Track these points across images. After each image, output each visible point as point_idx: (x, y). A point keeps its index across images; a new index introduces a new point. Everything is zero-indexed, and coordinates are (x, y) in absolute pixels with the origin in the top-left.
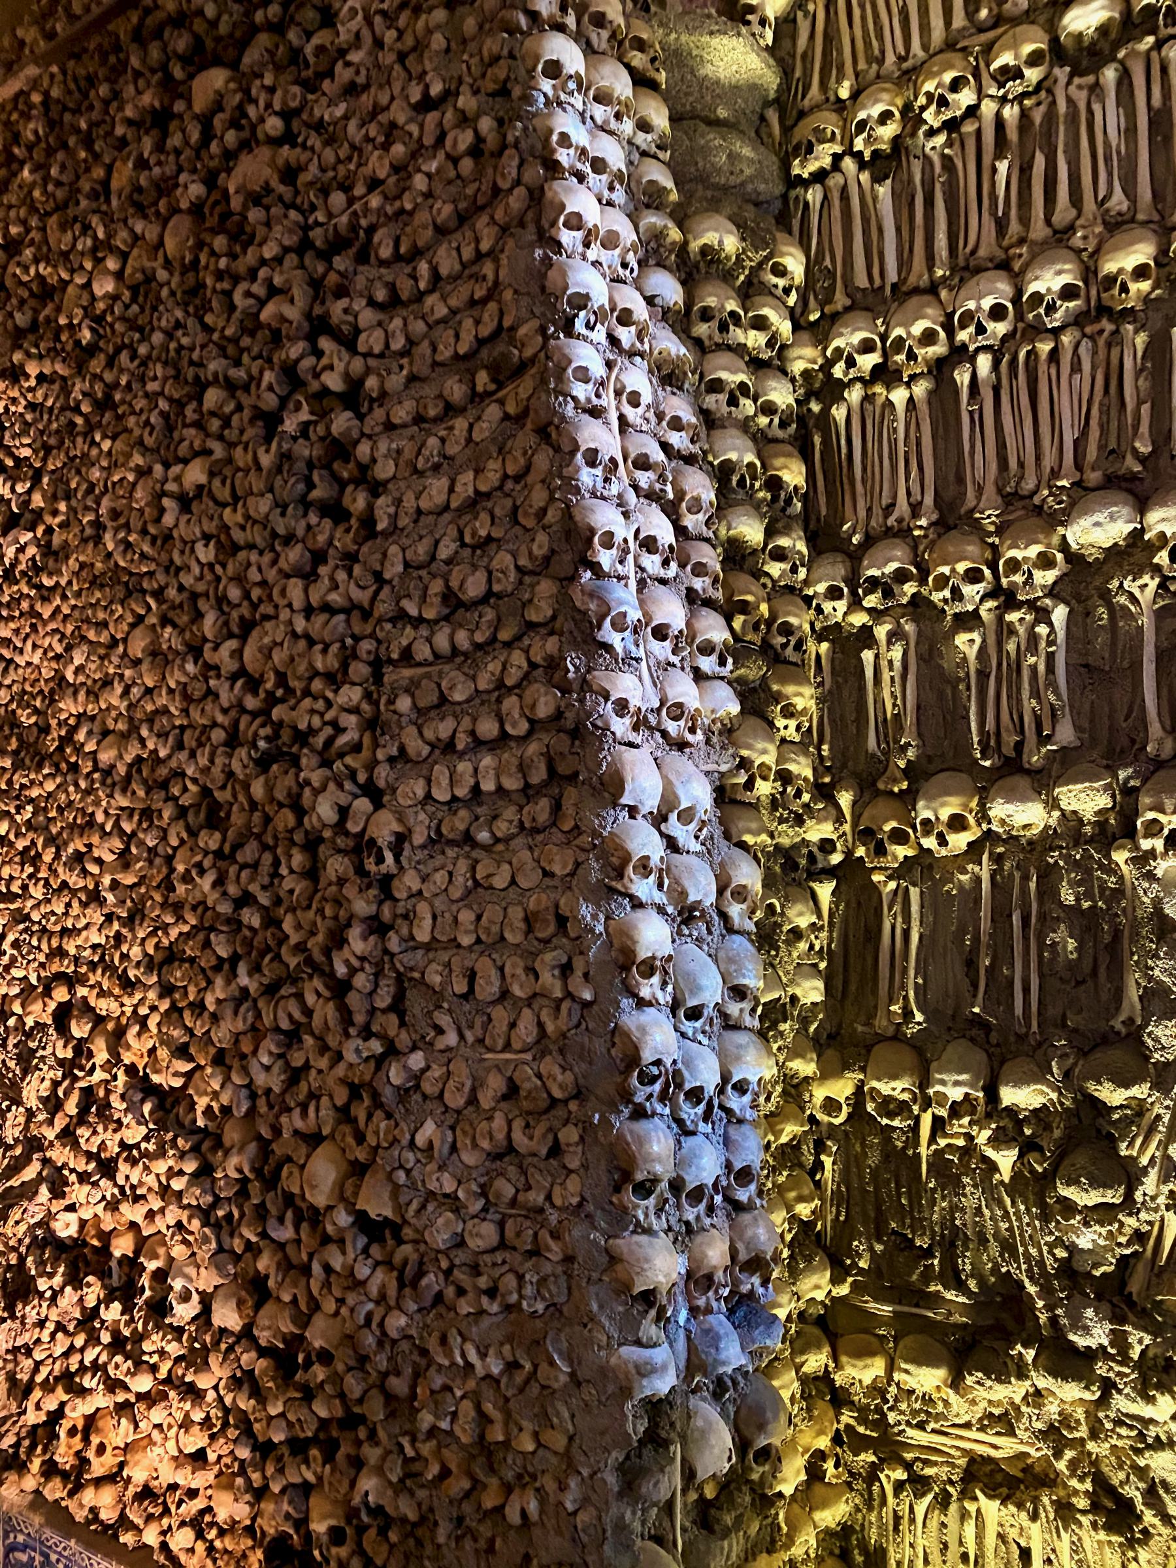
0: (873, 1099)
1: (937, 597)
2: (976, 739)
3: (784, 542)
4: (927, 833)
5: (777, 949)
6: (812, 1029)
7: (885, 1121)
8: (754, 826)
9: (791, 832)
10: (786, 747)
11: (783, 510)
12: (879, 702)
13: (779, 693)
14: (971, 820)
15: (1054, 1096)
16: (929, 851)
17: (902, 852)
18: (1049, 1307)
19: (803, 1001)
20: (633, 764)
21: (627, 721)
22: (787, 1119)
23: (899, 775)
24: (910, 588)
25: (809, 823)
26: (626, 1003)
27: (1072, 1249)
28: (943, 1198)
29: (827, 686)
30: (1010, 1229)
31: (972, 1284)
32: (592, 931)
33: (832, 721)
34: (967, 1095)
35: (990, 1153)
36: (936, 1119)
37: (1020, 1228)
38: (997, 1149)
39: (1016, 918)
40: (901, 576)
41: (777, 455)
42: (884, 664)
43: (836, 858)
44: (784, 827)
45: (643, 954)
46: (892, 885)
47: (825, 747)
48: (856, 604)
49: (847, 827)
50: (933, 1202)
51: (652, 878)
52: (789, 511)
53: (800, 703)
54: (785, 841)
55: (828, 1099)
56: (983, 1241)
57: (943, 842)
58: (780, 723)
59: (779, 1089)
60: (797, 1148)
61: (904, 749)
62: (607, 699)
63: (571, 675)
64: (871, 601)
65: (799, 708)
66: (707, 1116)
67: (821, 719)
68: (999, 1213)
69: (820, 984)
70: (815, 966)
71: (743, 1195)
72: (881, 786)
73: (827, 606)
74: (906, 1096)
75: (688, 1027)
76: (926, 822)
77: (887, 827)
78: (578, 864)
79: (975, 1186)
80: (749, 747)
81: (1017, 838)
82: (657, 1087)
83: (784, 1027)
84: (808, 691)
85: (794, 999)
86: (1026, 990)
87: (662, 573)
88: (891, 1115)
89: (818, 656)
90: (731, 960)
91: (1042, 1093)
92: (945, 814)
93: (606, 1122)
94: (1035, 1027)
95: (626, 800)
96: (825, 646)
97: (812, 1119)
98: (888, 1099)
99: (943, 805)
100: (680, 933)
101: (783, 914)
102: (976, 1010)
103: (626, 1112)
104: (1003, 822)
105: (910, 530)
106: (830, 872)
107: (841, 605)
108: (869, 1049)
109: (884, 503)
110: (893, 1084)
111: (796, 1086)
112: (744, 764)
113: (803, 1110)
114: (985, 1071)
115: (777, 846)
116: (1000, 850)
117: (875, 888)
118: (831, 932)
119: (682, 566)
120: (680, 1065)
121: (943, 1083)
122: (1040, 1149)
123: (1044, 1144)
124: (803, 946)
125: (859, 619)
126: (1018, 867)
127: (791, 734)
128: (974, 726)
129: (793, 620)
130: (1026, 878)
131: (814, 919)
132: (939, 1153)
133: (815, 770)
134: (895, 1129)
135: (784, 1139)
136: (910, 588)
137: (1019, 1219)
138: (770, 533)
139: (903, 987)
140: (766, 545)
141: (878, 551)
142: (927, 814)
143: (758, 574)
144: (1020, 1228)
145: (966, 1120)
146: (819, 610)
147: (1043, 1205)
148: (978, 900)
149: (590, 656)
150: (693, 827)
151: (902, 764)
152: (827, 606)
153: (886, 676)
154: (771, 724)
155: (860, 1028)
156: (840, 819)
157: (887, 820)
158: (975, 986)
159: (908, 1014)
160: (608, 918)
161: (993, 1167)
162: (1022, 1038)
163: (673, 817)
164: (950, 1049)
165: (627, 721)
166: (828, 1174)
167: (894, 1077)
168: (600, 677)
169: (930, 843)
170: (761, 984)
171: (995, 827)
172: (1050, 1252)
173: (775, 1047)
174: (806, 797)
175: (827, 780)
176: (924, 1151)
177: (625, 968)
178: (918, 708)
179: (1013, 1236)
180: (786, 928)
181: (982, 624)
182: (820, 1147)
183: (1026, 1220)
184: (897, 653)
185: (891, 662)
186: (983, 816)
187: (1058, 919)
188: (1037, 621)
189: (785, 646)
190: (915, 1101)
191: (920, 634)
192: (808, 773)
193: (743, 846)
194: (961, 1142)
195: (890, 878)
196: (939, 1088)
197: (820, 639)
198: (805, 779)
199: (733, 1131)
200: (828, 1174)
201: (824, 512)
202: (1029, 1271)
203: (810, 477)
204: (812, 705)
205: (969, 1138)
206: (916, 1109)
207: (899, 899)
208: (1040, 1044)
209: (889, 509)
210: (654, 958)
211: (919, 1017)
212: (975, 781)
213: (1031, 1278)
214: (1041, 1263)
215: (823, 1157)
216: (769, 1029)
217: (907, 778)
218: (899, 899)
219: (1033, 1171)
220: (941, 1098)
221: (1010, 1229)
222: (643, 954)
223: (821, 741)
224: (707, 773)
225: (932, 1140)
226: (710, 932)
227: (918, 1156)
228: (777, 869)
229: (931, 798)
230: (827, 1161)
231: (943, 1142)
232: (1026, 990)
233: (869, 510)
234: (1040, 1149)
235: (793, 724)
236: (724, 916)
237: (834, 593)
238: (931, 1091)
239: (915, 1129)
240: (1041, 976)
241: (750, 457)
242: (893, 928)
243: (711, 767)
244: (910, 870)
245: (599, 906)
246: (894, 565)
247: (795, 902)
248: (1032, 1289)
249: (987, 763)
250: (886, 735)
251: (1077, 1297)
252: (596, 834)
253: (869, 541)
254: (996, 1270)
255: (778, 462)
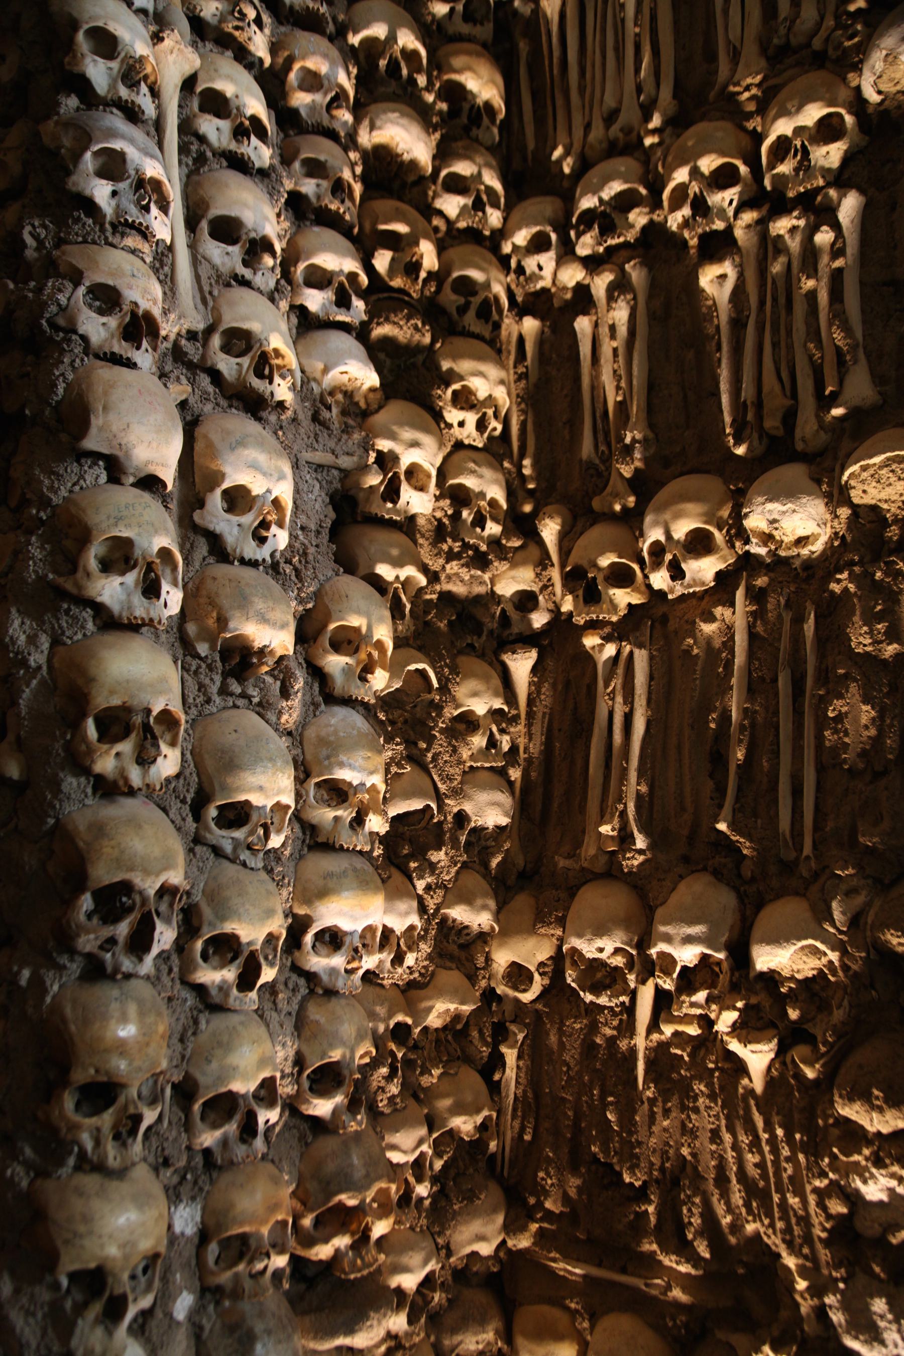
0: (574, 964)
1: (675, 220)
2: (728, 419)
3: (463, 168)
4: (657, 565)
5: (431, 740)
6: (495, 862)
7: (589, 997)
8: (395, 552)
9: (465, 574)
10: (462, 454)
11: (467, 129)
12: (596, 387)
13: (451, 371)
14: (719, 537)
15: (834, 956)
16: (661, 594)
17: (623, 597)
18: (817, 1290)
19: (477, 821)
20: (111, 385)
21: (113, 322)
22: (441, 994)
23: (621, 487)
24: (638, 218)
25: (499, 567)
26: (71, 783)
27: (854, 1199)
28: (666, 1113)
29: (533, 378)
30: (762, 1165)
31: (703, 1250)
32: (24, 663)
33: (538, 425)
34: (704, 958)
35: (735, 1046)
36: (660, 993)
37: (776, 1163)
38: (745, 1041)
39: (783, 681)
40: (625, 202)
41: (457, 53)
42: (604, 331)
43: (539, 620)
44: (453, 567)
45: (103, 700)
46: (610, 650)
47: (527, 462)
48: (567, 253)
49: (555, 574)
50: (652, 1119)
51: (131, 578)
52: (480, 133)
53: (481, 387)
54: (459, 589)
55: (514, 964)
56: (722, 1181)
57: (677, 573)
58: (453, 415)
59: (425, 948)
60: (464, 1034)
61: (628, 450)
62: (77, 284)
63: (30, 254)
64: (586, 245)
65: (482, 394)
66: (247, 980)
67: (523, 425)
68: (744, 1139)
69: (505, 798)
70: (502, 772)
71: (322, 1107)
72: (596, 504)
73: (530, 264)
74: (619, 961)
75: (225, 838)
76: (658, 550)
77: (605, 561)
78: (16, 553)
79: (712, 1097)
80: (393, 437)
81: (786, 561)
82: (123, 929)
83: (439, 856)
84: (493, 371)
85: (461, 818)
86: (797, 792)
87: (233, 146)
88: (596, 990)
89: (521, 340)
90: (322, 742)
91: (815, 952)
92: (682, 529)
93: (38, 985)
94: (807, 850)
95: (91, 443)
96: (530, 325)
97: (490, 995)
98: (596, 965)
99: (678, 516)
100: (224, 691)
101: (444, 689)
102: (722, 826)
103: (75, 968)
104: (767, 538)
105: (640, 140)
106: (530, 639)
107: (548, 260)
108: (572, 892)
109: (605, 108)
110: (599, 943)
111: (465, 947)
112: (386, 461)
113: (472, 978)
114: (730, 918)
115: (447, 597)
116: (761, 581)
117: (587, 658)
118: (529, 725)
119: (286, 158)
120: (197, 897)
121: (668, 939)
122: (811, 1040)
123: (818, 1032)
124: (479, 741)
125: (572, 275)
126: (788, 605)
127: (469, 433)
128: (725, 399)
129: (477, 275)
130: (799, 620)
131: (498, 704)
132: (663, 1046)
133: (511, 494)
134: (602, 1008)
135: (434, 1020)
136: (638, 218)
137: (775, 1151)
138: (442, 155)
139: (620, 799)
140: (436, 171)
141: (593, 175)
142: (655, 534)
143: (429, 211)
144: (776, 1163)
145: (701, 996)
146: (520, 270)
147: (810, 1128)
148: (729, 664)
149: (61, 223)
150: (249, 519)
151: (627, 471)
152: (530, 264)
153: (607, 347)
154: (438, 416)
155: (562, 863)
156: (543, 561)
157: (602, 553)
158: (721, 790)
159: (625, 838)
160: (56, 642)
161: (740, 1067)
162: (788, 868)
163: (216, 500)
164: (682, 887)
165: (113, 322)
166: (511, 1073)
167: (600, 931)
168: (74, 255)
169: (660, 580)
170: (377, 780)
171: (758, 549)
172: (821, 1205)
173: (420, 885)
174: (493, 528)
175: (528, 508)
176: (640, 1042)
177: (76, 725)
178: (652, 387)
179: (764, 1176)
180: (451, 712)
181: (739, 249)
182: (500, 1034)
183: (786, 1152)
184: (620, 314)
185: (613, 328)
186: (739, 533)
187: (846, 676)
188: (813, 229)
189: (463, 310)
190: (630, 965)
191: (653, 286)
192: (497, 493)
193: (378, 584)
194: (693, 1030)
195: (607, 639)
196: (662, 947)
197: (521, 310)
198: (493, 503)
199: (316, 1013)
200: (511, 1073)
201: (531, 145)
202: (788, 1230)
203: (511, 94)
204: (501, 394)
205: (707, 1023)
206: (631, 978)
207: (620, 671)
208: (816, 875)
209: (611, 118)
210: (126, 710)
211: (641, 842)
212: (726, 483)
213: (790, 1245)
214: (804, 1220)
215: (504, 1049)
216: (412, 856)
217: (635, 492)
218: (620, 671)
219: (799, 1076)
220: (668, 961)
221: (762, 1165)
222: (103, 700)
223: (522, 456)
224: (319, 468)
225: (654, 1026)
226: (285, 693)
227: (633, 1051)
228: (442, 625)
229: (660, 509)
230: (510, 1055)
231: (668, 1030)
232: (797, 792)
233: (588, 127)
234: (811, 1040)
235: (471, 418)
236: (317, 674)
237: (539, 244)
238: (653, 952)
239: (630, 1010)
240: (821, 769)
241: (407, 39)
242: (611, 714)
243: (320, 457)
244: (637, 627)
245: (41, 623)
246: (616, 187)
247: (466, 677)
248: (791, 1262)
249: (740, 451)
250: (607, 434)
251: (861, 1280)
252: (45, 503)
253: (584, 166)
254: (736, 1227)
255: (458, 61)
